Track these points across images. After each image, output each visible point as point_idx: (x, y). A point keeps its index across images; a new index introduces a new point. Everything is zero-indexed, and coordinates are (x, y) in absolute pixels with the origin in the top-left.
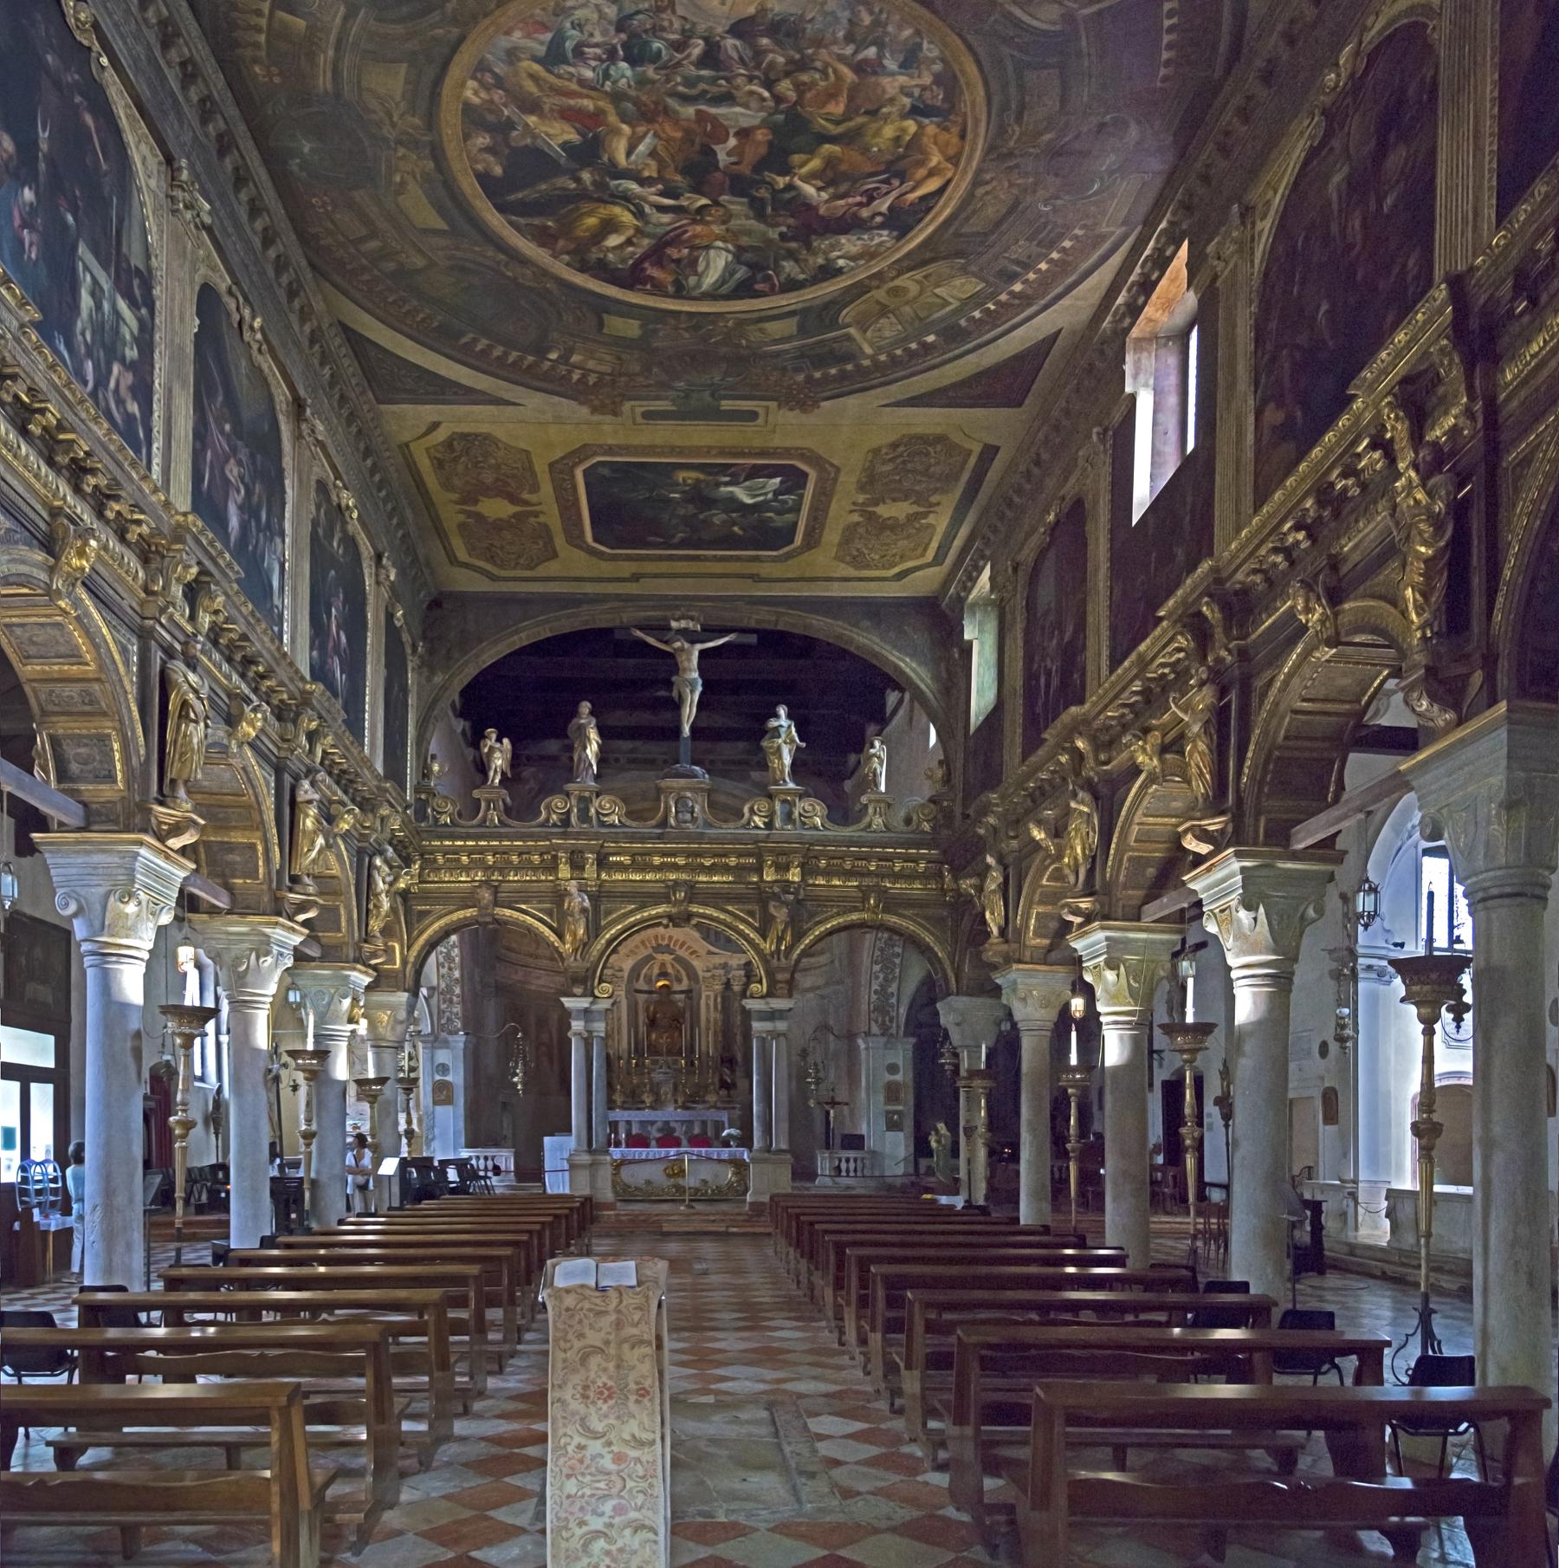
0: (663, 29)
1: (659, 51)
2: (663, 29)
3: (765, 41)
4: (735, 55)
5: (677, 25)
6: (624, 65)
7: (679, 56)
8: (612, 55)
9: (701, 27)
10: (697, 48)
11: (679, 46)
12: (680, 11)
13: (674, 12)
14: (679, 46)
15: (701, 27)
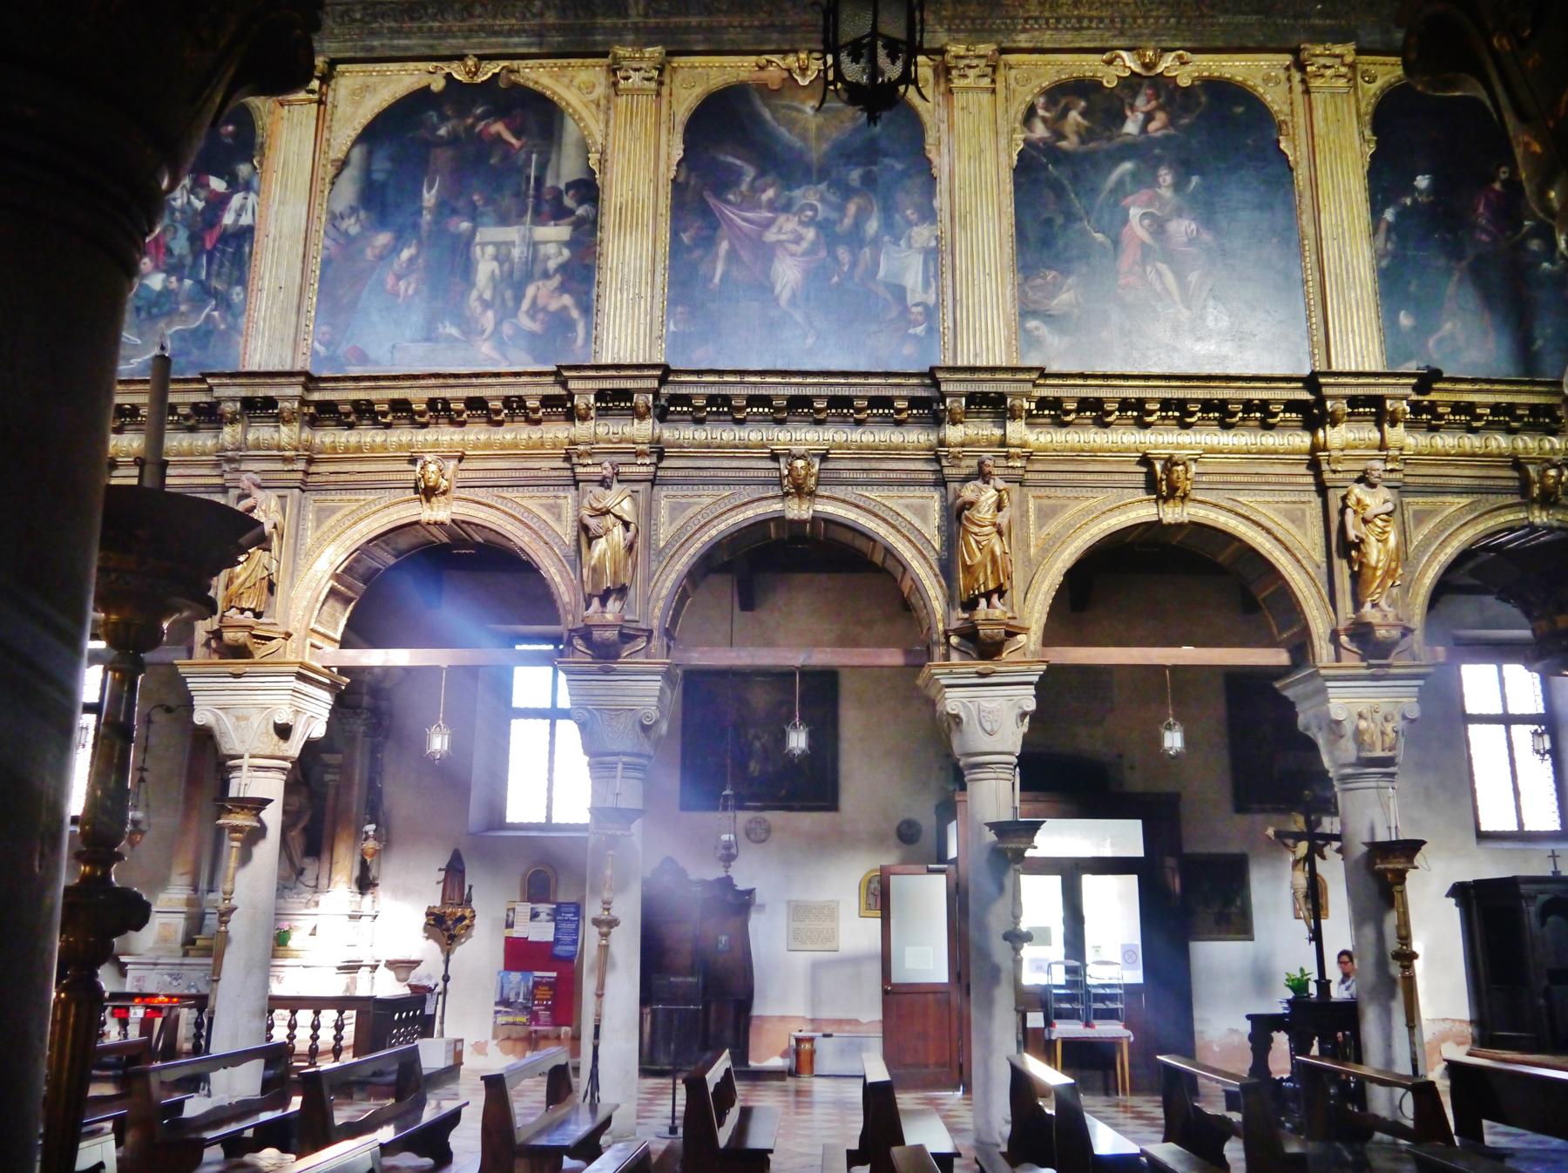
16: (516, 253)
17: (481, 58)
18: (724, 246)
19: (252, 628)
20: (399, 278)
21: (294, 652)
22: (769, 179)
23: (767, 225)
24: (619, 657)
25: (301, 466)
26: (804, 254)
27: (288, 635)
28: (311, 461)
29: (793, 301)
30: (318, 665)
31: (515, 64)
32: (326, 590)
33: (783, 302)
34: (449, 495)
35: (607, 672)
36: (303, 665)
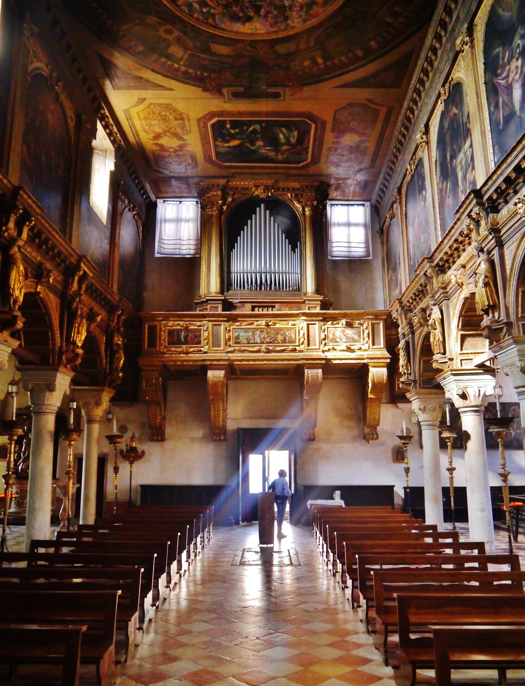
0: (273, 17)
1: (275, 10)
2: (273, 17)
3: (241, 15)
4: (250, 10)
5: (269, 19)
6: (287, 4)
7: (269, 9)
8: (291, 8)
9: (261, 19)
10: (262, 12)
11: (268, 13)
12: (268, 23)
13: (270, 23)
14: (268, 13)
15: (261, 19)
16: (463, 162)
17: (443, 86)
18: (501, 100)
19: (437, 361)
20: (449, 197)
21: (456, 365)
22: (506, 48)
23: (508, 76)
24: (499, 340)
25: (441, 291)
26: (520, 77)
27: (451, 360)
28: (445, 288)
29: (521, 108)
30: (473, 367)
31: (450, 78)
32: (459, 336)
33: (518, 113)
34: (464, 284)
35: (502, 348)
36: (451, 370)
